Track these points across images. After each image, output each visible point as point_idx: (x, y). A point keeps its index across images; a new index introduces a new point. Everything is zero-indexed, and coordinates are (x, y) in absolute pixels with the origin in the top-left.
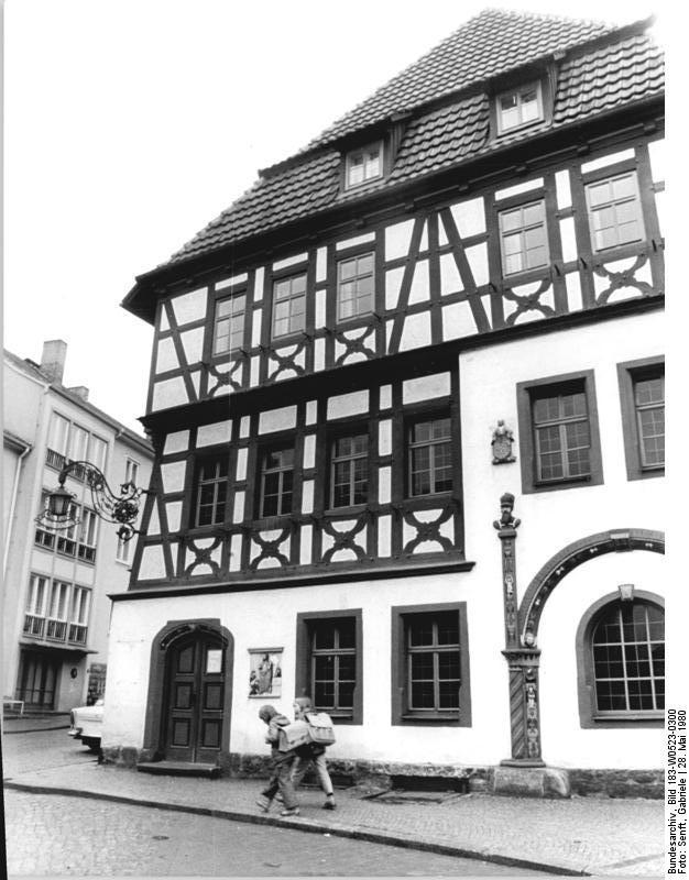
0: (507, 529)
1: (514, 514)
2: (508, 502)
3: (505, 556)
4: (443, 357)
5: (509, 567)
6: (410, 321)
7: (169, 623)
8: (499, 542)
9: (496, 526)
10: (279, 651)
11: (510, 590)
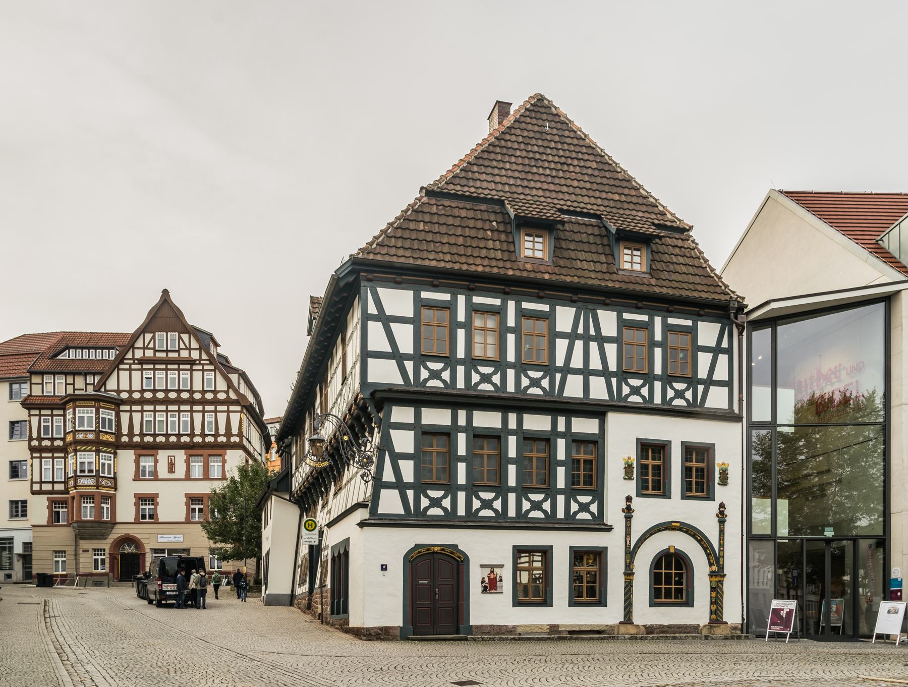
0: (628, 511)
1: (632, 507)
2: (629, 499)
3: (626, 526)
4: (598, 411)
5: (628, 533)
6: (570, 378)
7: (417, 546)
8: (624, 520)
9: (623, 511)
10: (501, 566)
11: (628, 543)
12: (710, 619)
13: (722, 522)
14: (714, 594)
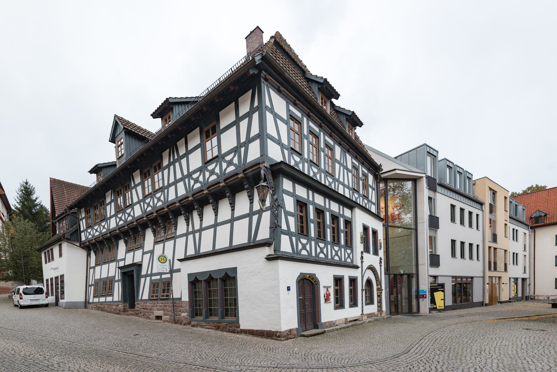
2: (362, 253)
10: (330, 287)
12: (378, 310)
13: (381, 266)
14: (379, 298)
